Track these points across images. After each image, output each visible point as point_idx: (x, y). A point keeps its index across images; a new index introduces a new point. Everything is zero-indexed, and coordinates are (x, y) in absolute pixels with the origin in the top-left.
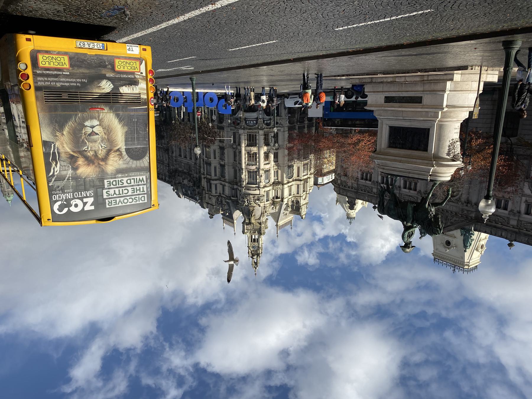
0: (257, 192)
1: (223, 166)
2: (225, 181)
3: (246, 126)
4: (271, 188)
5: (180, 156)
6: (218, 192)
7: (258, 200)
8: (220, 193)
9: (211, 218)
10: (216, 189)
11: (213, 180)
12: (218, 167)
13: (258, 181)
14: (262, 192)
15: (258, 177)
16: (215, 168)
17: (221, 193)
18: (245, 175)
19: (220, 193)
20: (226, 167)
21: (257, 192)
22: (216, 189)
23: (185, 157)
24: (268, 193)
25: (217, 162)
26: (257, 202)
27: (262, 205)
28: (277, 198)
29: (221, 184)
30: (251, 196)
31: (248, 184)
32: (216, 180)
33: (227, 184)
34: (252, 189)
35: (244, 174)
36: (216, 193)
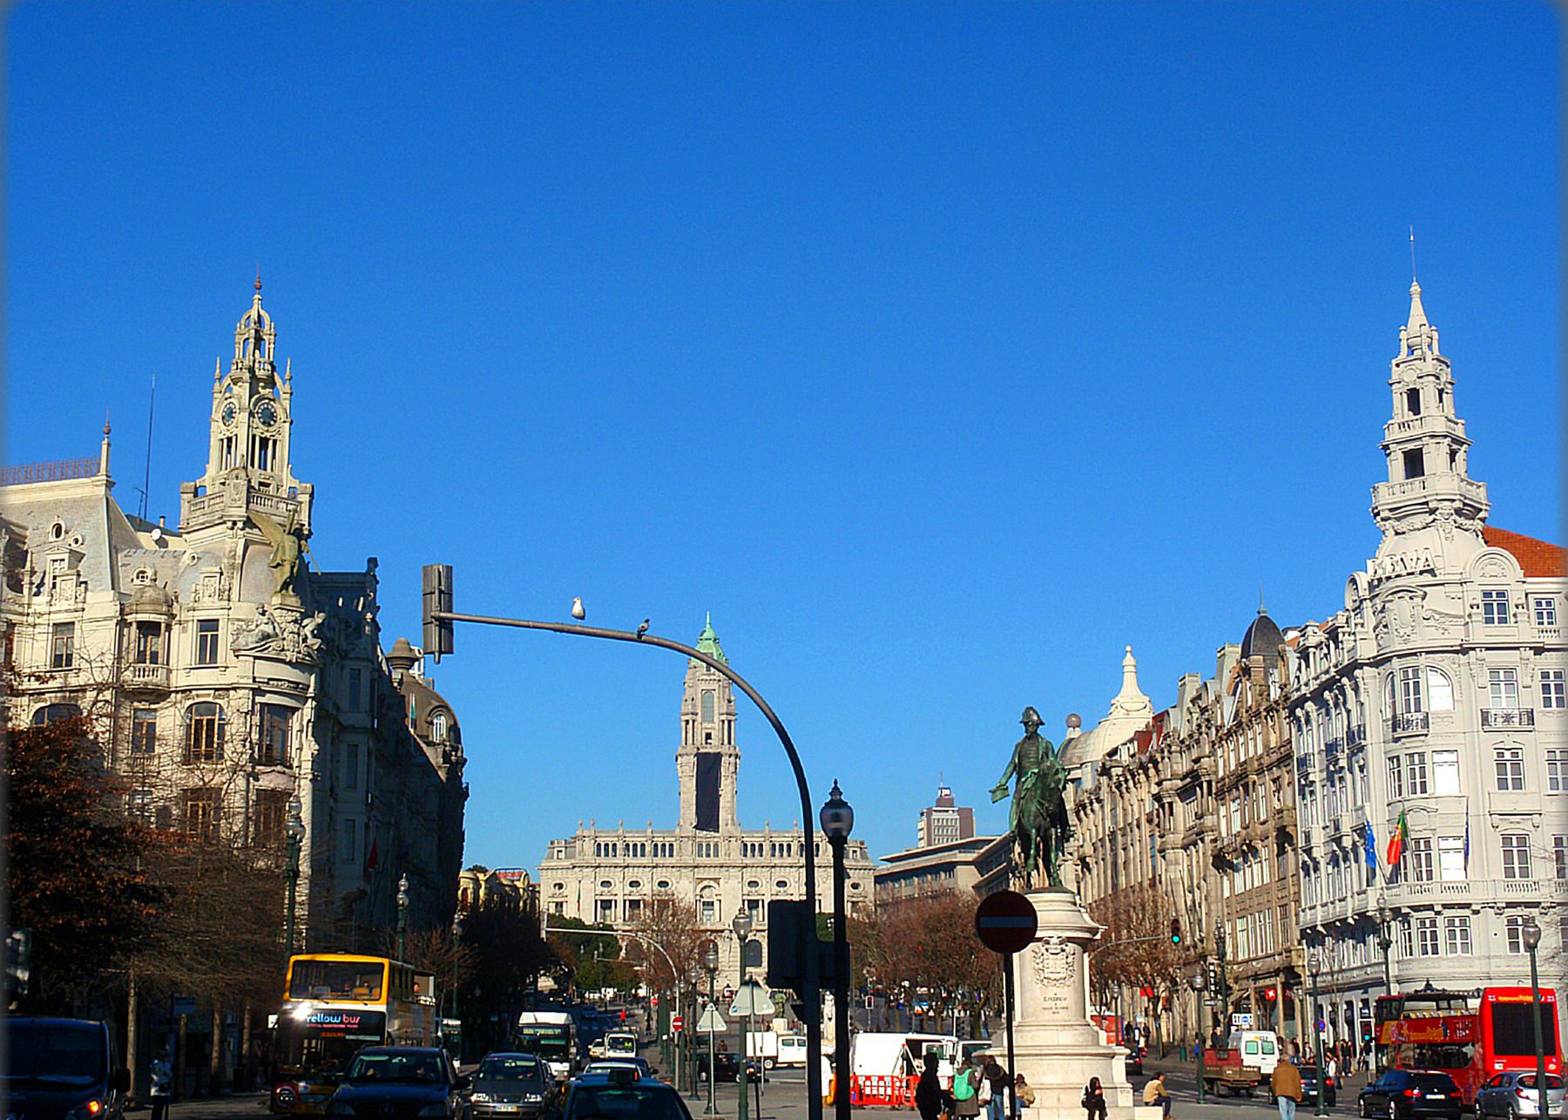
0: (265, 670)
4: (179, 680)
7: (266, 637)
9: (373, 562)
10: (355, 688)
13: (256, 719)
14: (238, 671)
15: (255, 737)
18: (303, 748)
19: (342, 668)
21: (265, 670)
22: (355, 688)
26: (269, 629)
27: (244, 609)
28: (149, 629)
29: (338, 709)
30: (290, 656)
31: (294, 710)
32: (353, 729)
35: (307, 755)
36: (356, 674)
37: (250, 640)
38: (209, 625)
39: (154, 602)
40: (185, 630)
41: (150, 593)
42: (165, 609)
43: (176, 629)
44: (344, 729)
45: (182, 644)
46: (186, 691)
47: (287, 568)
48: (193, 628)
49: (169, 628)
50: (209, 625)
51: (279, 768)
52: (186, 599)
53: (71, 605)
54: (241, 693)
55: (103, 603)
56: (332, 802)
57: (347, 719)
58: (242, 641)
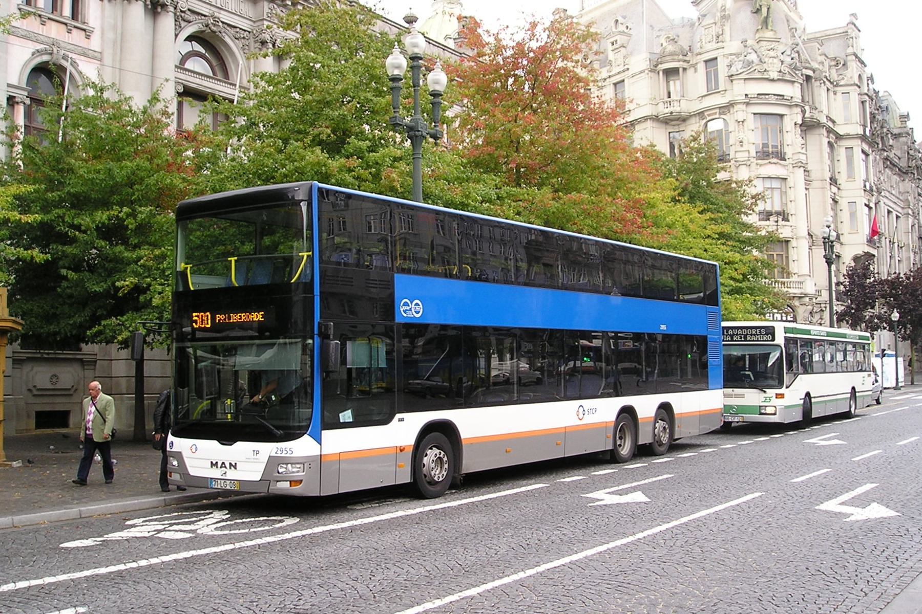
0: (755, 88)
1: (833, 181)
2: (830, 131)
3: (796, 303)
5: (897, 217)
6: (839, 94)
8: (835, 93)
11: (857, 137)
12: (842, 179)
16: (851, 176)
17: (831, 93)
19: (835, 93)
20: (828, 175)
21: (755, 88)
23: (889, 212)
24: (712, 88)
25: (843, 193)
26: (753, 57)
28: (671, 73)
29: (834, 122)
30: (774, 75)
32: (848, 137)
33: (823, 120)
34: (773, 100)
37: (738, 67)
38: (711, 62)
39: (671, 54)
40: (696, 71)
41: (670, 48)
42: (681, 57)
43: (690, 72)
44: (839, 137)
45: (696, 80)
46: (701, 114)
47: (764, 10)
48: (701, 67)
49: (685, 69)
50: (711, 62)
51: (774, 160)
52: (696, 51)
53: (621, 68)
54: (737, 107)
55: (640, 61)
56: (834, 189)
57: (841, 130)
58: (733, 68)
